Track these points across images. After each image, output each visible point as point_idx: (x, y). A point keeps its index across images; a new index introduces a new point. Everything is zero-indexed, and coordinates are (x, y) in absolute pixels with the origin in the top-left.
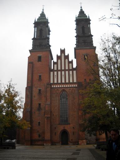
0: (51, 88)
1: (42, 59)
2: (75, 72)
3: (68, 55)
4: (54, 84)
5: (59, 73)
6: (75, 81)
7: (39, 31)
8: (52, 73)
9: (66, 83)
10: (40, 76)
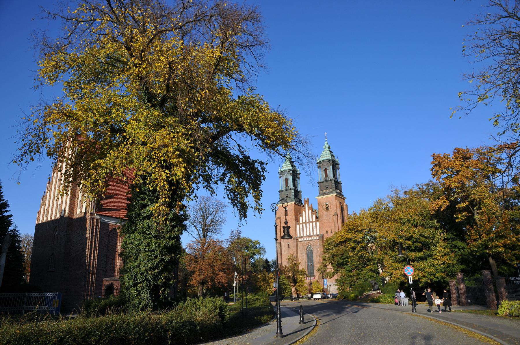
2: (318, 223)
4: (301, 237)
5: (304, 225)
6: (318, 233)
8: (298, 226)
9: (310, 236)
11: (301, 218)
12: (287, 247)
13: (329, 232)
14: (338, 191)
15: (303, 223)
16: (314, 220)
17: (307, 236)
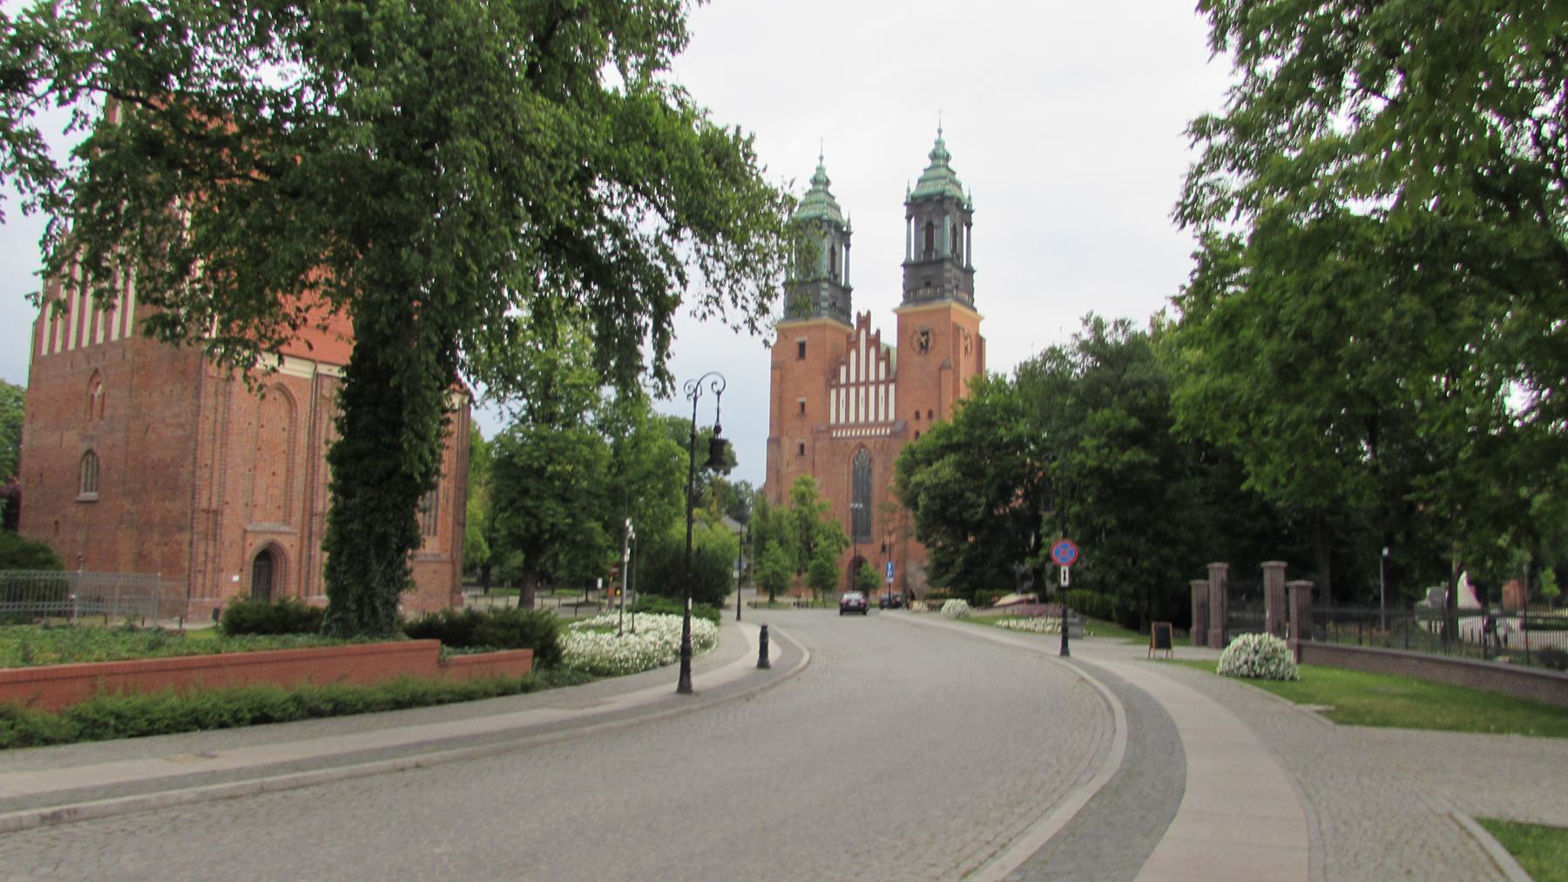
0: (832, 439)
2: (892, 387)
3: (878, 332)
4: (838, 426)
5: (853, 391)
6: (892, 417)
8: (833, 393)
9: (867, 425)
10: (803, 405)
11: (843, 370)
12: (797, 450)
13: (923, 415)
14: (966, 297)
15: (848, 385)
16: (882, 376)
17: (857, 425)
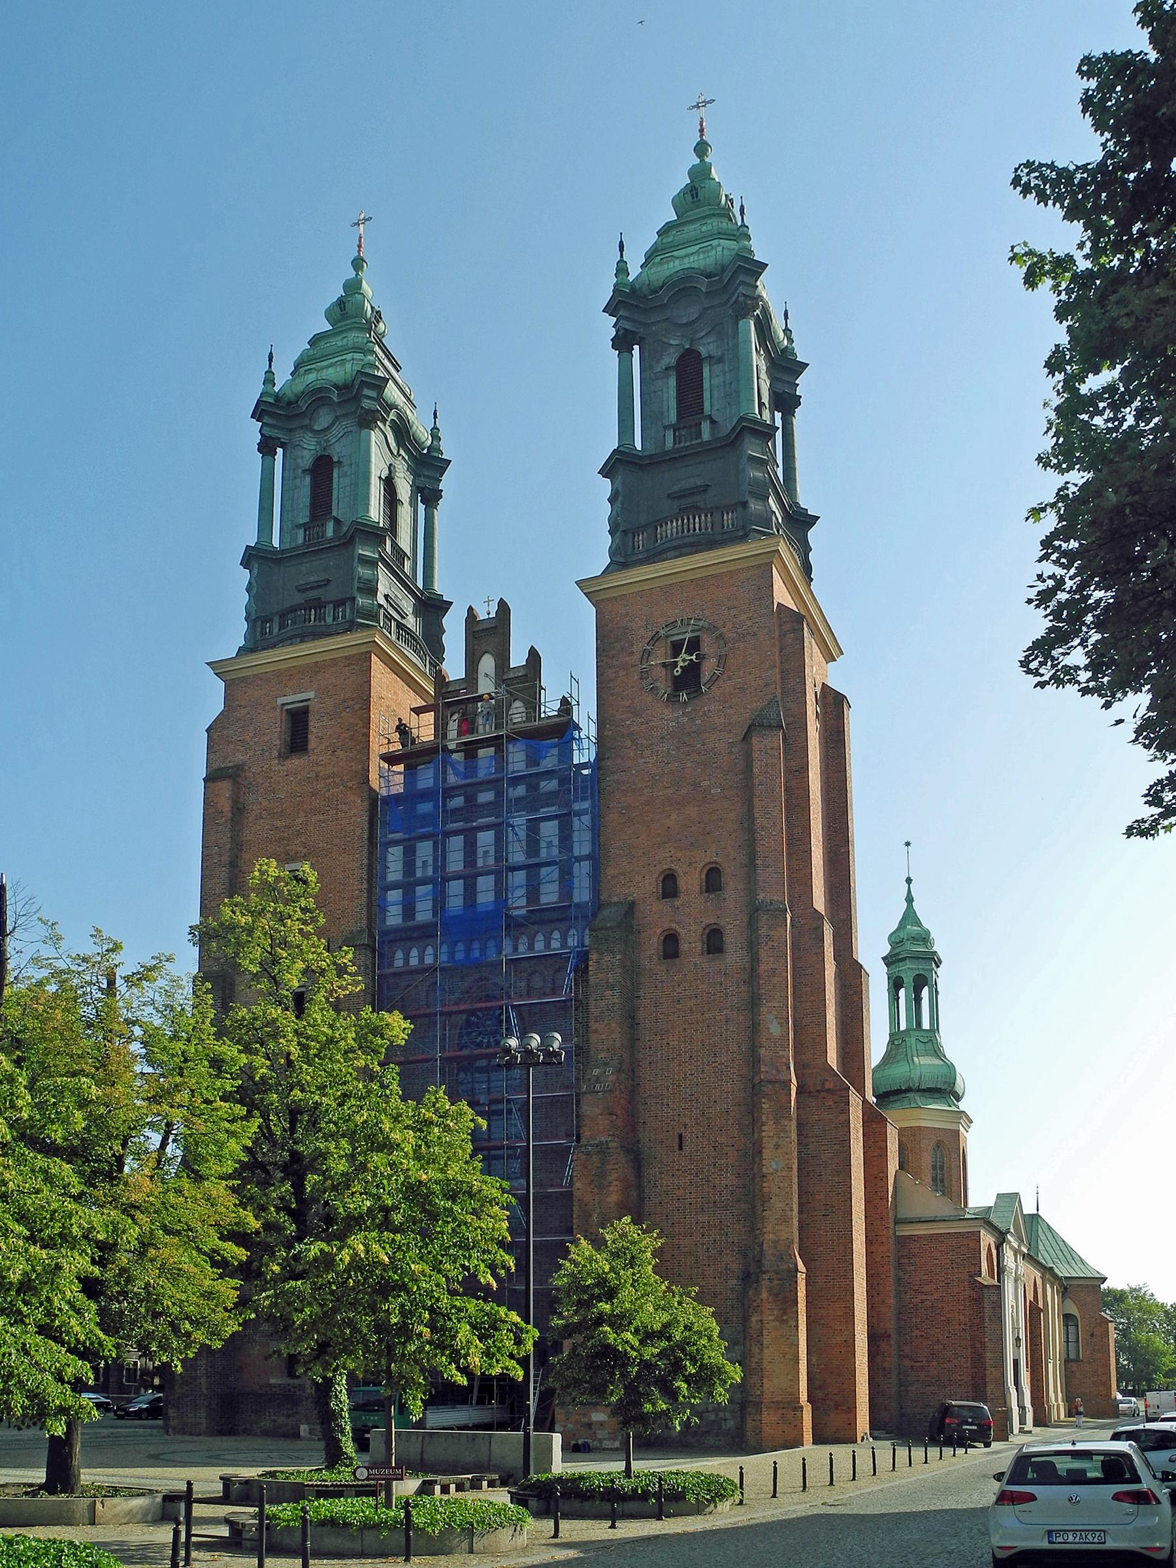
1: (314, 726)
3: (534, 657)
7: (308, 479)
13: (690, 881)
